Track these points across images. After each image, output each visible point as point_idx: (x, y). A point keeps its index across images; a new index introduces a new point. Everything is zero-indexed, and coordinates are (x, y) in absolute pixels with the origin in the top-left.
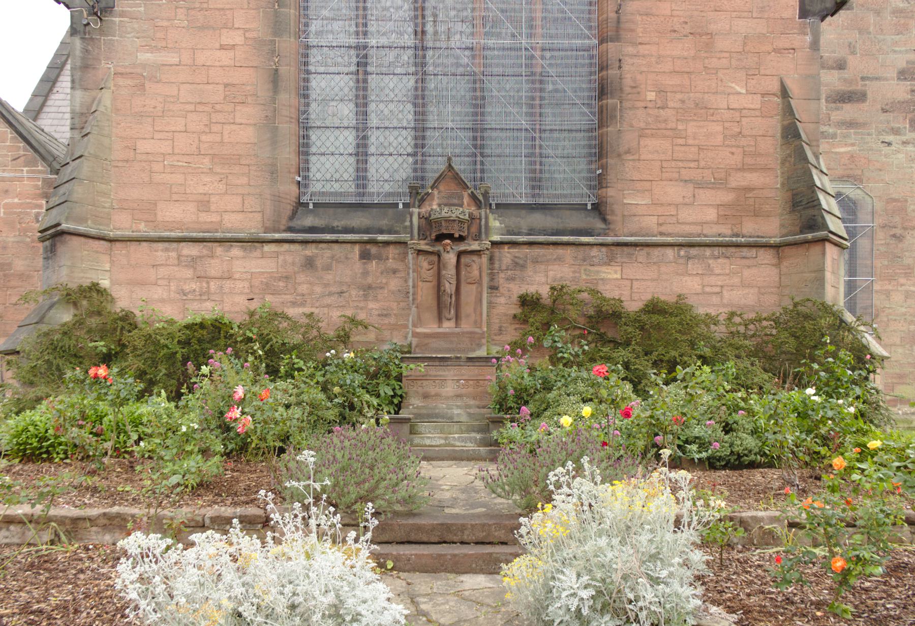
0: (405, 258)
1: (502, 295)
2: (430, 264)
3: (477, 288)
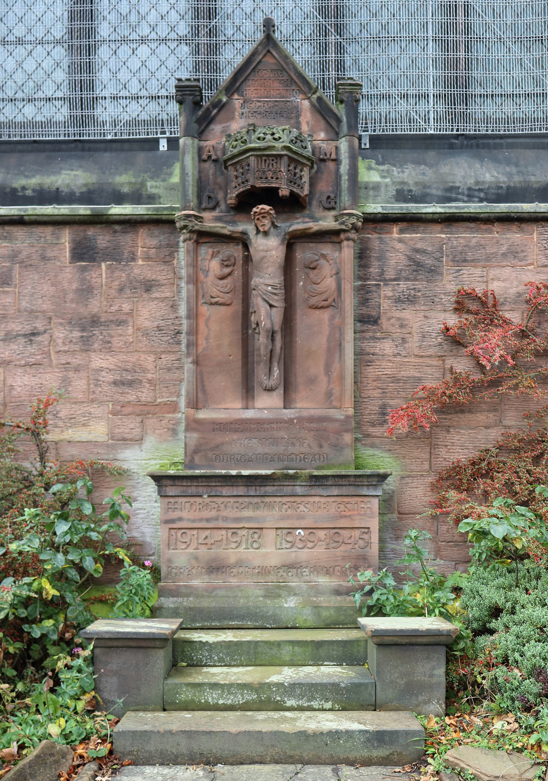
0: (171, 255)
1: (387, 335)
2: (224, 263)
3: (332, 318)
